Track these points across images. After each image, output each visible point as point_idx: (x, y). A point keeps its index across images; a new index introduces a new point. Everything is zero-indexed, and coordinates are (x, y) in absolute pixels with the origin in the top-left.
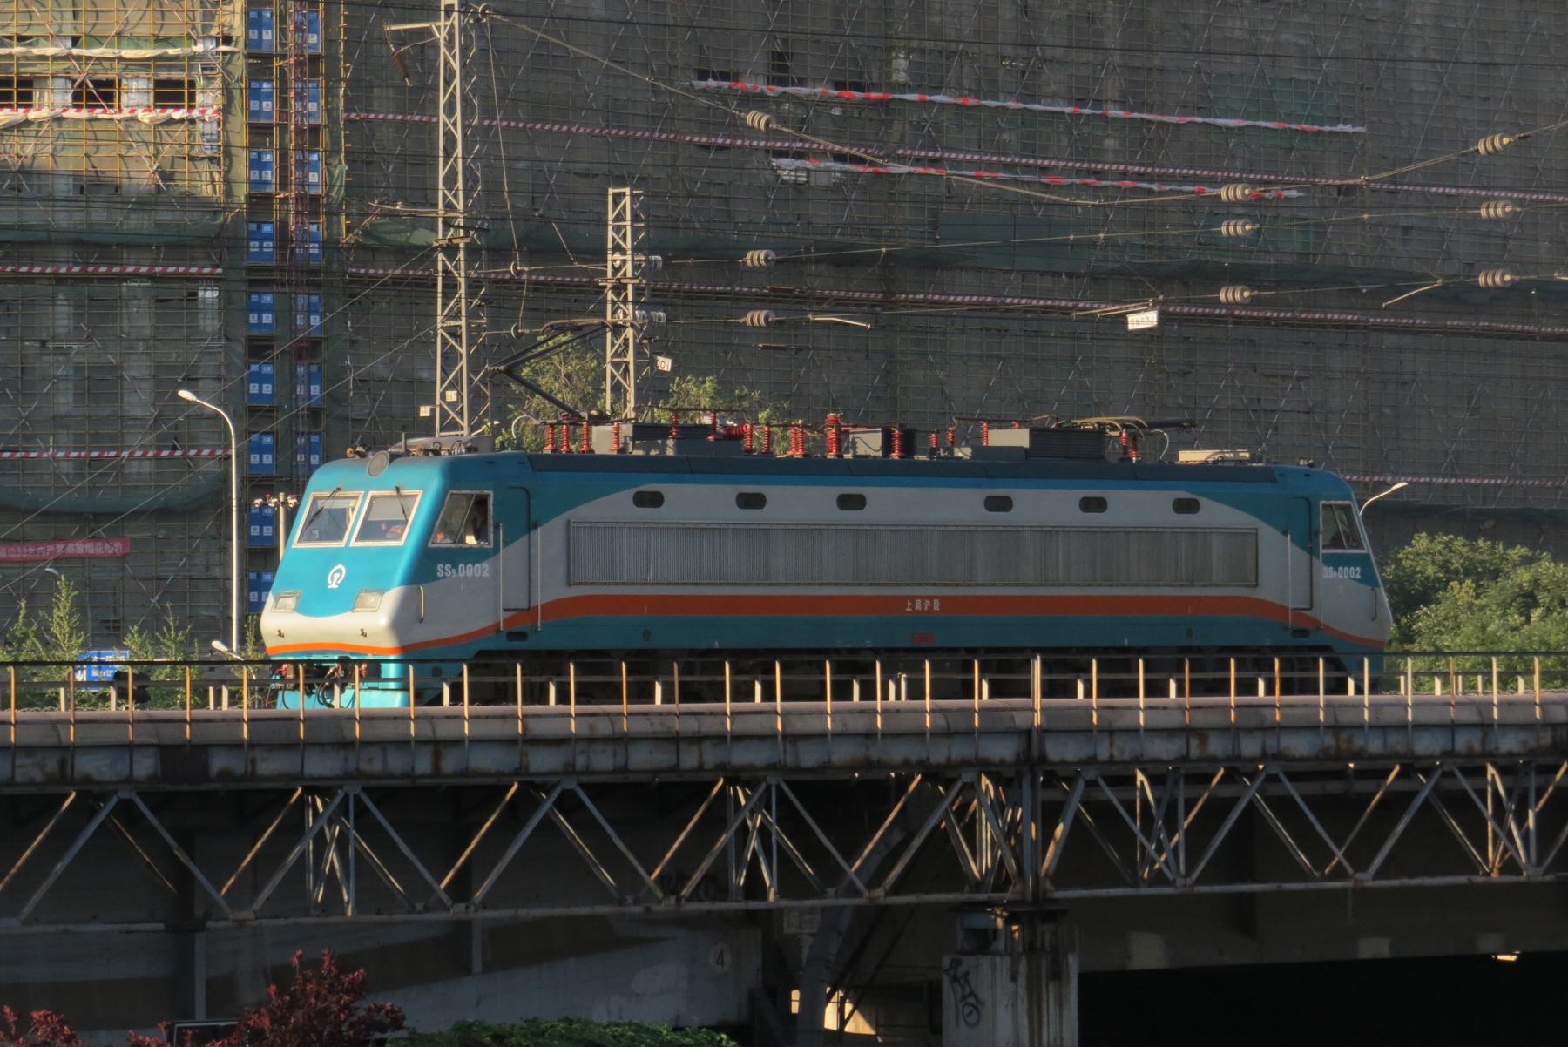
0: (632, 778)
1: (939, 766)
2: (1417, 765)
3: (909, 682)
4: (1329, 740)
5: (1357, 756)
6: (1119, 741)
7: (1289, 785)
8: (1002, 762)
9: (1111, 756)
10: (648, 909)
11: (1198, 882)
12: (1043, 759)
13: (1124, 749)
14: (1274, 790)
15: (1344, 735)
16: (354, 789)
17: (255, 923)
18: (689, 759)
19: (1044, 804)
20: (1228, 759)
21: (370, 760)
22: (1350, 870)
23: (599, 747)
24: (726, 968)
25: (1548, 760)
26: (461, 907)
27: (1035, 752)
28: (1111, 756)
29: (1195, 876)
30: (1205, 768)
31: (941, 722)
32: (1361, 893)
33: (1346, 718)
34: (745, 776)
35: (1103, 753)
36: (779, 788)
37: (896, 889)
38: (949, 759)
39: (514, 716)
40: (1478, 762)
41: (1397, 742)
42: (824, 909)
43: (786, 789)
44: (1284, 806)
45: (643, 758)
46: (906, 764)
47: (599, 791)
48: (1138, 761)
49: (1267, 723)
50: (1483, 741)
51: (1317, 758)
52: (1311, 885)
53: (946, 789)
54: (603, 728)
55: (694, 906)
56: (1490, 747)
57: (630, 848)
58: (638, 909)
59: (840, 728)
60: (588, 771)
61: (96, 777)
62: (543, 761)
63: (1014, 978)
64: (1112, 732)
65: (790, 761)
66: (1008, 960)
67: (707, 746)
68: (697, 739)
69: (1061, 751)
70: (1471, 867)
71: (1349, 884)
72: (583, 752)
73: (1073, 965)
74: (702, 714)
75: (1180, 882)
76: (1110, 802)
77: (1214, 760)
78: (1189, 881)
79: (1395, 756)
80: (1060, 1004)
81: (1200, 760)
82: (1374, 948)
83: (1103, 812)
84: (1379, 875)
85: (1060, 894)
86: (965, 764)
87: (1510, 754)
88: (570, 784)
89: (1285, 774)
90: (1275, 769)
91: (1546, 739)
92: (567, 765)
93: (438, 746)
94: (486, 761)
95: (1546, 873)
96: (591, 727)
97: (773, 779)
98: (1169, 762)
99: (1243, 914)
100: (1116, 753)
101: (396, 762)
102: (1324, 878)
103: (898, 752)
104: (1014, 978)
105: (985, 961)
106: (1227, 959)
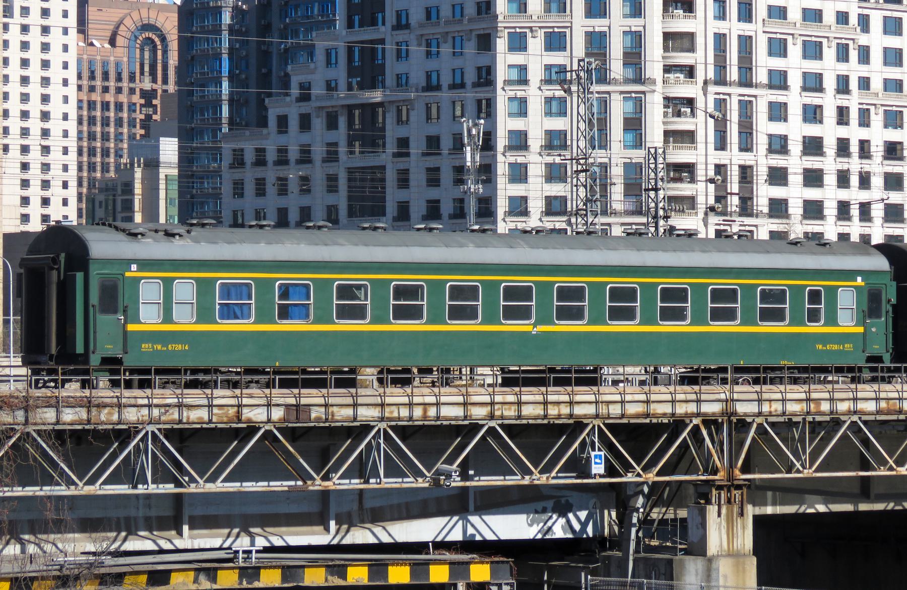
8: (714, 414)
9: (770, 412)
11: (815, 471)
12: (734, 413)
16: (383, 425)
17: (333, 488)
18: (553, 411)
21: (392, 412)
22: (895, 466)
23: (506, 407)
28: (770, 412)
29: (814, 469)
34: (585, 421)
35: (766, 408)
36: (599, 426)
45: (527, 411)
46: (664, 415)
60: (502, 417)
61: (254, 419)
62: (479, 413)
63: (719, 515)
67: (562, 406)
69: (741, 408)
71: (894, 473)
72: (499, 409)
77: (823, 414)
78: (811, 471)
88: (493, 424)
90: (855, 418)
93: (425, 405)
100: (773, 409)
101: (404, 412)
104: (719, 515)
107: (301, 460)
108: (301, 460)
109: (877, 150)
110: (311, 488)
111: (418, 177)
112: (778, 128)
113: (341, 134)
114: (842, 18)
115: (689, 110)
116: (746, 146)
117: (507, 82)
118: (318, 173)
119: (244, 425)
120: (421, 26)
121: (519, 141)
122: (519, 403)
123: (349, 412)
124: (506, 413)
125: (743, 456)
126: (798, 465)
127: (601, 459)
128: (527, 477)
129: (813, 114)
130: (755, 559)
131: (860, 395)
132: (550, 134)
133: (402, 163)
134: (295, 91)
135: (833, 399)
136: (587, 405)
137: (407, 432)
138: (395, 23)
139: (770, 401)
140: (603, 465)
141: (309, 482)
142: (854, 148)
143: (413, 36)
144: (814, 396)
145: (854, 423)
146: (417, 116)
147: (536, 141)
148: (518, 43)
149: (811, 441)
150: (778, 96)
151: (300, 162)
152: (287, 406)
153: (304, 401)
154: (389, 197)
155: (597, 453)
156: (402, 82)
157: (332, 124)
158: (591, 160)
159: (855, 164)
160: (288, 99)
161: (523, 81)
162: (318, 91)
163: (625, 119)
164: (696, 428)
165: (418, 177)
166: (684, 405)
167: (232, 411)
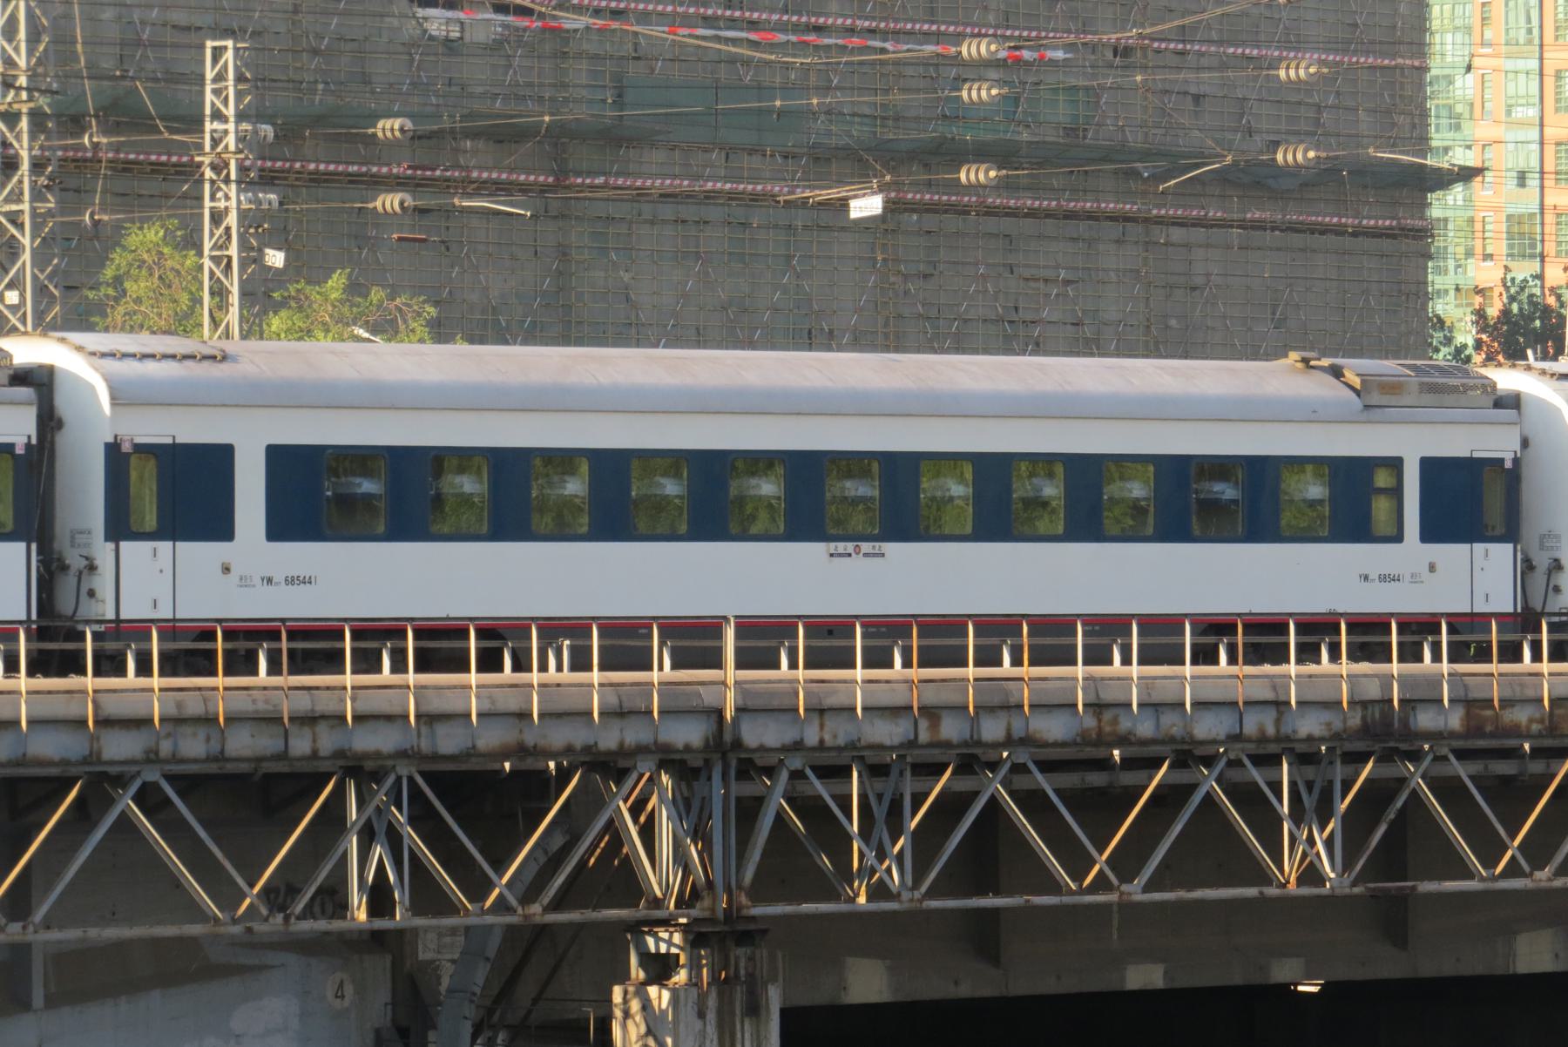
0: (230, 768)
1: (609, 753)
2: (1198, 752)
3: (572, 649)
4: (1090, 722)
5: (1123, 740)
6: (831, 723)
7: (1039, 777)
9: (822, 741)
10: (249, 930)
11: (930, 894)
12: (738, 744)
13: (837, 732)
14: (1021, 782)
15: (1107, 715)
18: (301, 745)
19: (739, 800)
20: (965, 744)
23: (188, 729)
24: (347, 1002)
25: (1359, 746)
26: (15, 927)
27: (728, 737)
28: (822, 741)
29: (924, 889)
30: (936, 755)
31: (613, 700)
32: (1127, 907)
33: (1108, 695)
34: (369, 765)
36: (411, 779)
37: (557, 905)
38: (621, 744)
39: (84, 692)
40: (1273, 748)
41: (1171, 724)
42: (467, 929)
43: (420, 780)
44: (1033, 803)
45: (242, 743)
46: (569, 750)
47: (189, 784)
48: (852, 746)
49: (1013, 701)
50: (1278, 722)
51: (1075, 744)
52: (1066, 900)
53: (618, 784)
54: (194, 707)
55: (307, 925)
56: (1286, 729)
57: (227, 855)
58: (237, 929)
59: (487, 706)
60: (175, 759)
62: (119, 747)
64: (822, 712)
65: (425, 746)
68: (308, 720)
69: (760, 735)
70: (1264, 878)
71: (1113, 897)
72: (169, 735)
73: (774, 999)
74: (317, 688)
75: (906, 895)
76: (820, 797)
77: (948, 745)
78: (917, 895)
79: (1172, 740)
81: (931, 745)
82: (1144, 976)
83: (811, 809)
84: (1147, 888)
85: (757, 911)
86: (641, 750)
87: (1310, 739)
88: (152, 775)
89: (1036, 763)
90: (1023, 757)
91: (1355, 721)
92: (147, 752)
94: (50, 746)
95: (1354, 884)
96: (179, 705)
97: (404, 770)
98: (892, 748)
99: (984, 935)
100: (827, 737)
102: (1081, 891)
103: (561, 736)
104: (701, 1015)
106: (965, 991)
125: (755, 856)
166: (616, 724)
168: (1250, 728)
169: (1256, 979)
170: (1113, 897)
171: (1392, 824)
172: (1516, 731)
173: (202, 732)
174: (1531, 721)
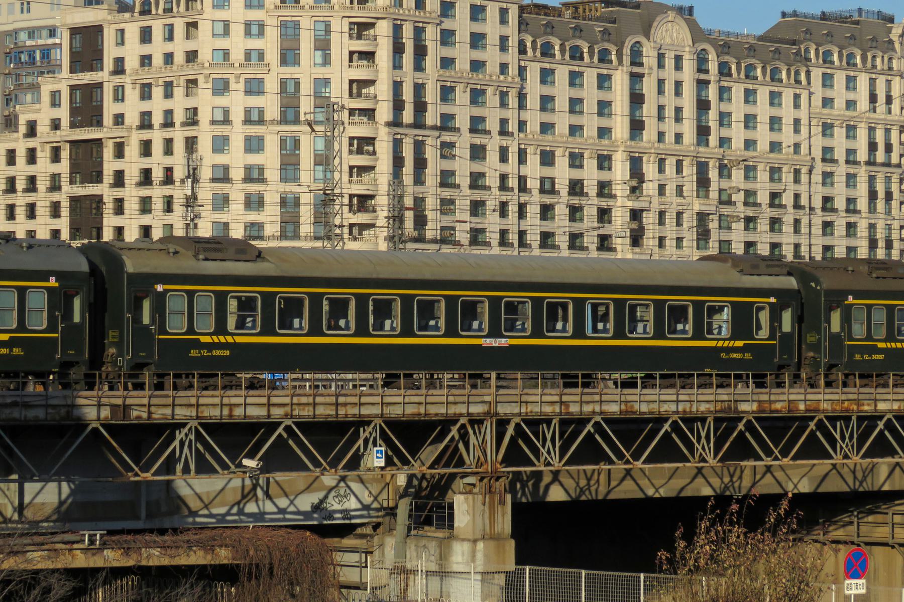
4: (623, 407)
11: (564, 465)
12: (497, 414)
15: (629, 404)
16: (194, 423)
17: (152, 478)
18: (342, 411)
21: (202, 412)
23: (301, 407)
35: (523, 410)
43: (383, 424)
45: (320, 411)
46: (437, 414)
50: (691, 407)
62: (277, 412)
66: (480, 496)
67: (349, 407)
69: (503, 409)
75: (556, 465)
77: (572, 414)
79: (651, 413)
80: (503, 515)
86: (461, 415)
87: (702, 412)
88: (288, 422)
90: (598, 418)
93: (230, 405)
105: (470, 496)
107: (124, 455)
108: (124, 455)
109: (533, 184)
110: (132, 479)
111: (132, 205)
112: (447, 165)
113: (64, 167)
114: (504, 67)
115: (370, 148)
116: (419, 180)
117: (213, 122)
118: (43, 199)
119: (73, 423)
120: (135, 72)
121: (222, 176)
122: (315, 404)
123: (168, 411)
124: (302, 413)
126: (549, 459)
127: (381, 453)
128: (318, 470)
129: (477, 152)
130: (513, 542)
131: (604, 398)
132: (248, 169)
133: (118, 193)
134: (23, 129)
135: (601, 402)
136: (370, 407)
137: (215, 429)
138: (112, 68)
139: (527, 403)
140: (383, 459)
141: (130, 474)
142: (513, 182)
143: (128, 80)
144: (565, 398)
145: (597, 424)
146: (132, 150)
147: (237, 174)
148: (222, 87)
149: (561, 437)
150: (447, 137)
151: (26, 191)
152: (113, 407)
153: (129, 401)
154: (105, 222)
155: (379, 448)
156: (119, 119)
157: (56, 157)
158: (337, 191)
159: (513, 199)
160: (15, 135)
161: (226, 121)
162: (43, 128)
163: (315, 155)
164: (463, 426)
165: (132, 205)
167: (63, 411)
168: (680, 409)
169: (696, 494)
170: (631, 466)
171: (732, 443)
172: (777, 411)
173: (307, 409)
174: (782, 407)
